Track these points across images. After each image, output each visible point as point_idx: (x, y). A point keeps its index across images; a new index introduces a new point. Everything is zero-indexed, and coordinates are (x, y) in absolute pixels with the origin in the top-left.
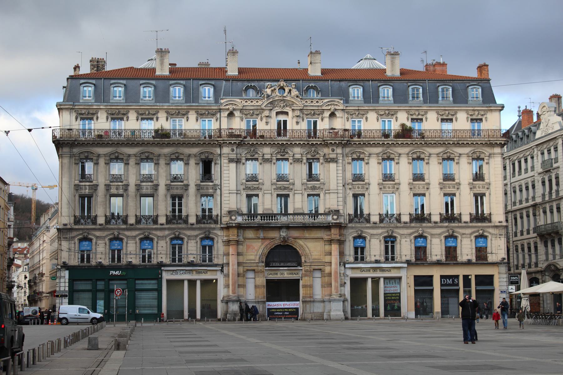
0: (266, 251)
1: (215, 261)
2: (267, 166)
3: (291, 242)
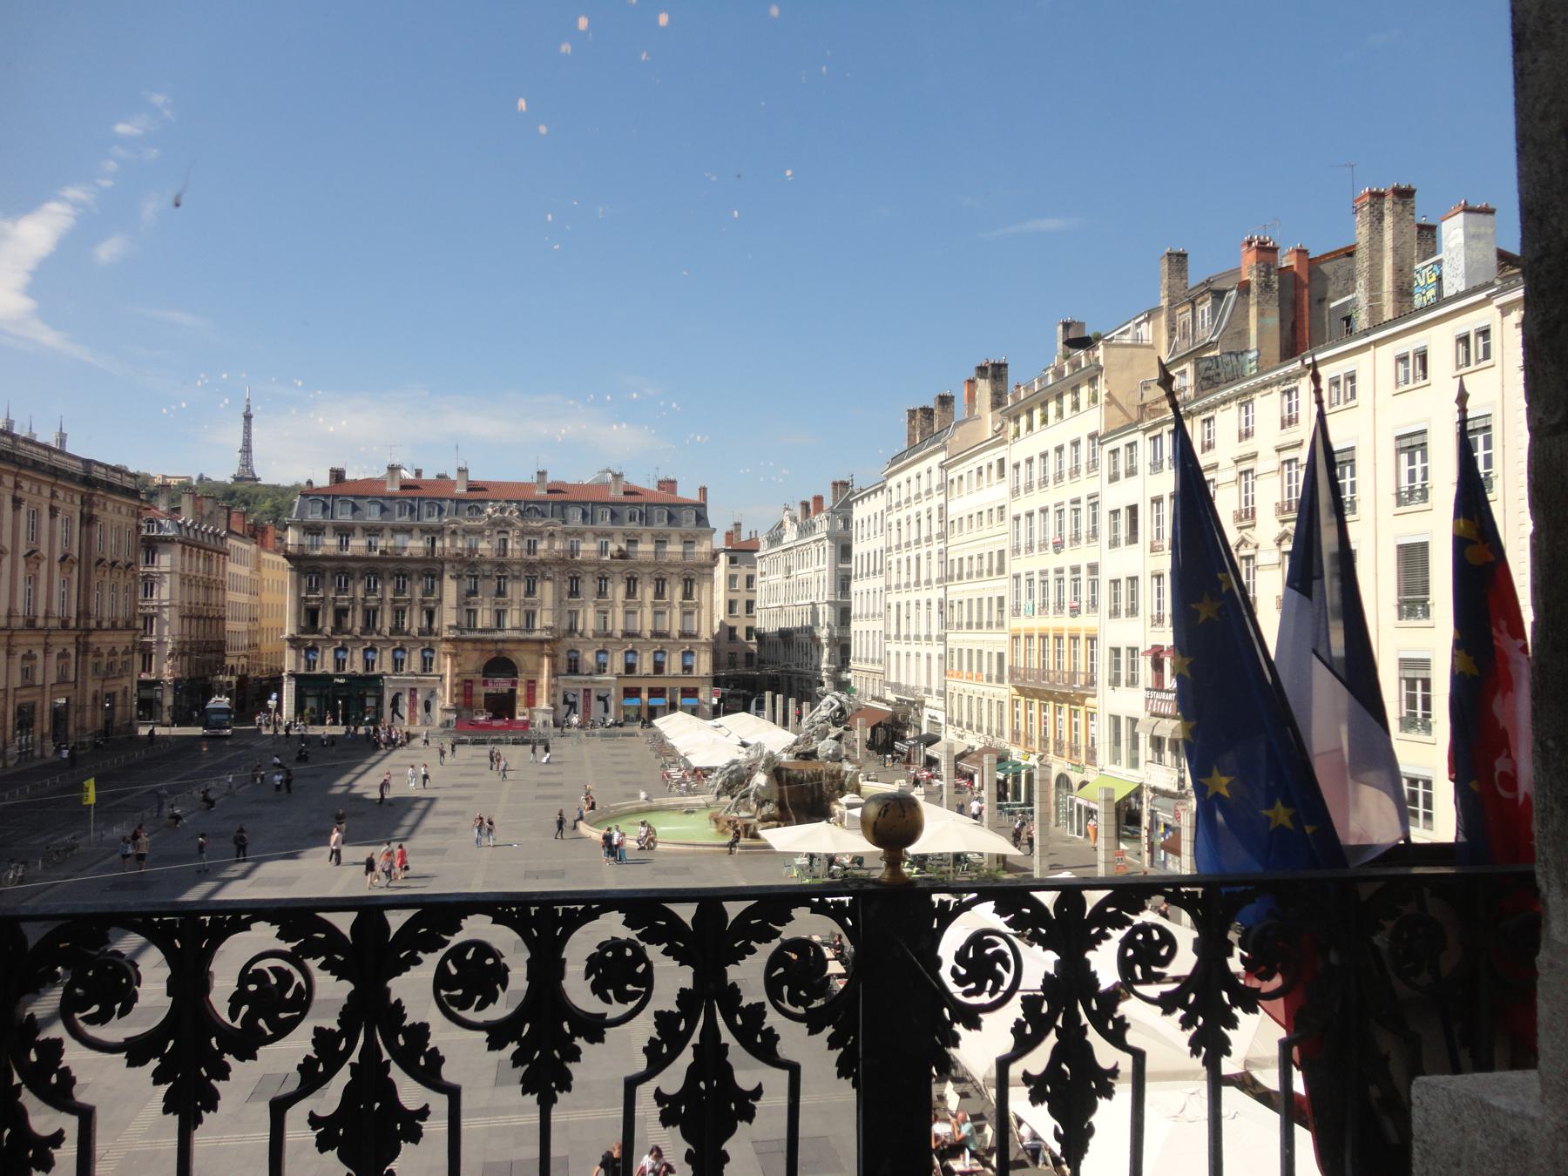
0: (484, 662)
1: (435, 671)
2: (487, 581)
3: (506, 655)
